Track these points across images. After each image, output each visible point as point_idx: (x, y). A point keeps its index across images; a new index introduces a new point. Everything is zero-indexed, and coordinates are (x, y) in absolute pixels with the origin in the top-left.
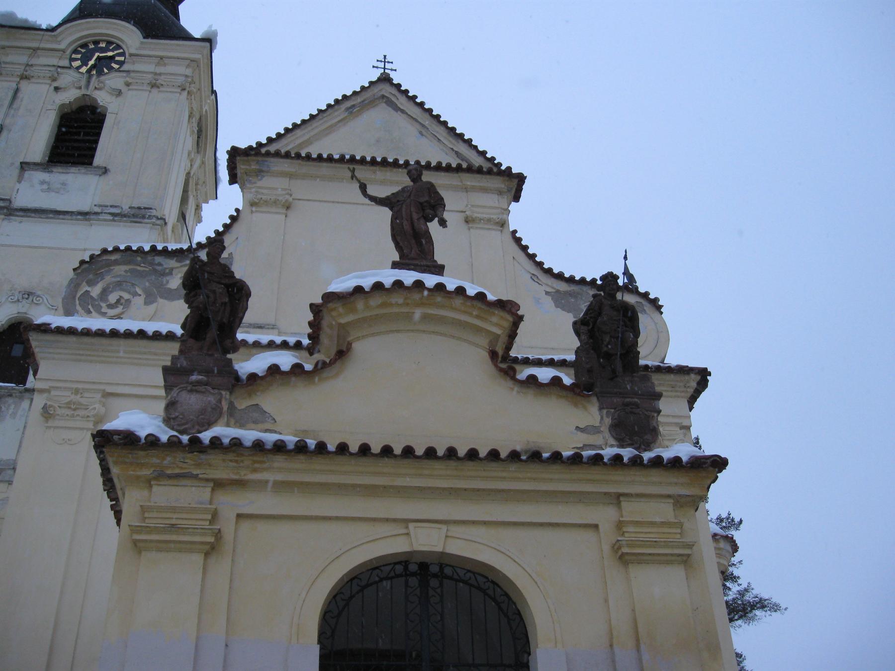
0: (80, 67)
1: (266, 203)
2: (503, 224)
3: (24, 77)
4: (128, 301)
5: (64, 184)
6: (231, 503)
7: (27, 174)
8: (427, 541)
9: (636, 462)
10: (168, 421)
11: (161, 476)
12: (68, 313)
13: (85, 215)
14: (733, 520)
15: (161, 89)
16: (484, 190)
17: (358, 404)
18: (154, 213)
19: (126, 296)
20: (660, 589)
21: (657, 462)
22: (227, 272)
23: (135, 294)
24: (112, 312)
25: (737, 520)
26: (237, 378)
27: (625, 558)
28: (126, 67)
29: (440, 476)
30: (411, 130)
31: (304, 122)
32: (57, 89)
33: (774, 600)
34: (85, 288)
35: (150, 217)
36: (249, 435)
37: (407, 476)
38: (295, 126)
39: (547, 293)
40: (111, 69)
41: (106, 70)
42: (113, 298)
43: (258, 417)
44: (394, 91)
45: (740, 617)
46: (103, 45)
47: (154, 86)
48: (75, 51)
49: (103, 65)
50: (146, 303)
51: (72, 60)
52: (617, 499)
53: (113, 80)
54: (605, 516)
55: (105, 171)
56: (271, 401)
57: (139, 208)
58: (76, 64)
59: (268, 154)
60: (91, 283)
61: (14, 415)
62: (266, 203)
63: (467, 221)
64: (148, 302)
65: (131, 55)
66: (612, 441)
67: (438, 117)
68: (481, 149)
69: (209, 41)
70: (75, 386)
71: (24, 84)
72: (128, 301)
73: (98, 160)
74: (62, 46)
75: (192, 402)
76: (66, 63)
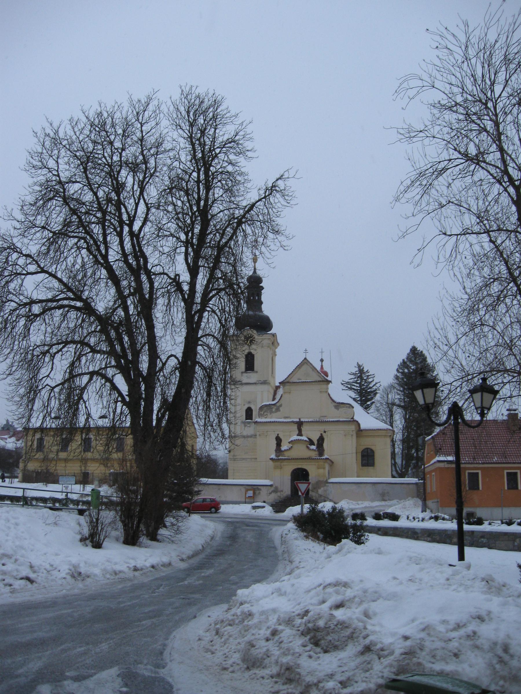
2: (327, 392)
6: (282, 464)
8: (300, 467)
10: (276, 456)
13: (255, 384)
17: (293, 454)
43: (284, 455)
49: (251, 341)
53: (253, 346)
54: (317, 464)
55: (257, 372)
73: (255, 369)
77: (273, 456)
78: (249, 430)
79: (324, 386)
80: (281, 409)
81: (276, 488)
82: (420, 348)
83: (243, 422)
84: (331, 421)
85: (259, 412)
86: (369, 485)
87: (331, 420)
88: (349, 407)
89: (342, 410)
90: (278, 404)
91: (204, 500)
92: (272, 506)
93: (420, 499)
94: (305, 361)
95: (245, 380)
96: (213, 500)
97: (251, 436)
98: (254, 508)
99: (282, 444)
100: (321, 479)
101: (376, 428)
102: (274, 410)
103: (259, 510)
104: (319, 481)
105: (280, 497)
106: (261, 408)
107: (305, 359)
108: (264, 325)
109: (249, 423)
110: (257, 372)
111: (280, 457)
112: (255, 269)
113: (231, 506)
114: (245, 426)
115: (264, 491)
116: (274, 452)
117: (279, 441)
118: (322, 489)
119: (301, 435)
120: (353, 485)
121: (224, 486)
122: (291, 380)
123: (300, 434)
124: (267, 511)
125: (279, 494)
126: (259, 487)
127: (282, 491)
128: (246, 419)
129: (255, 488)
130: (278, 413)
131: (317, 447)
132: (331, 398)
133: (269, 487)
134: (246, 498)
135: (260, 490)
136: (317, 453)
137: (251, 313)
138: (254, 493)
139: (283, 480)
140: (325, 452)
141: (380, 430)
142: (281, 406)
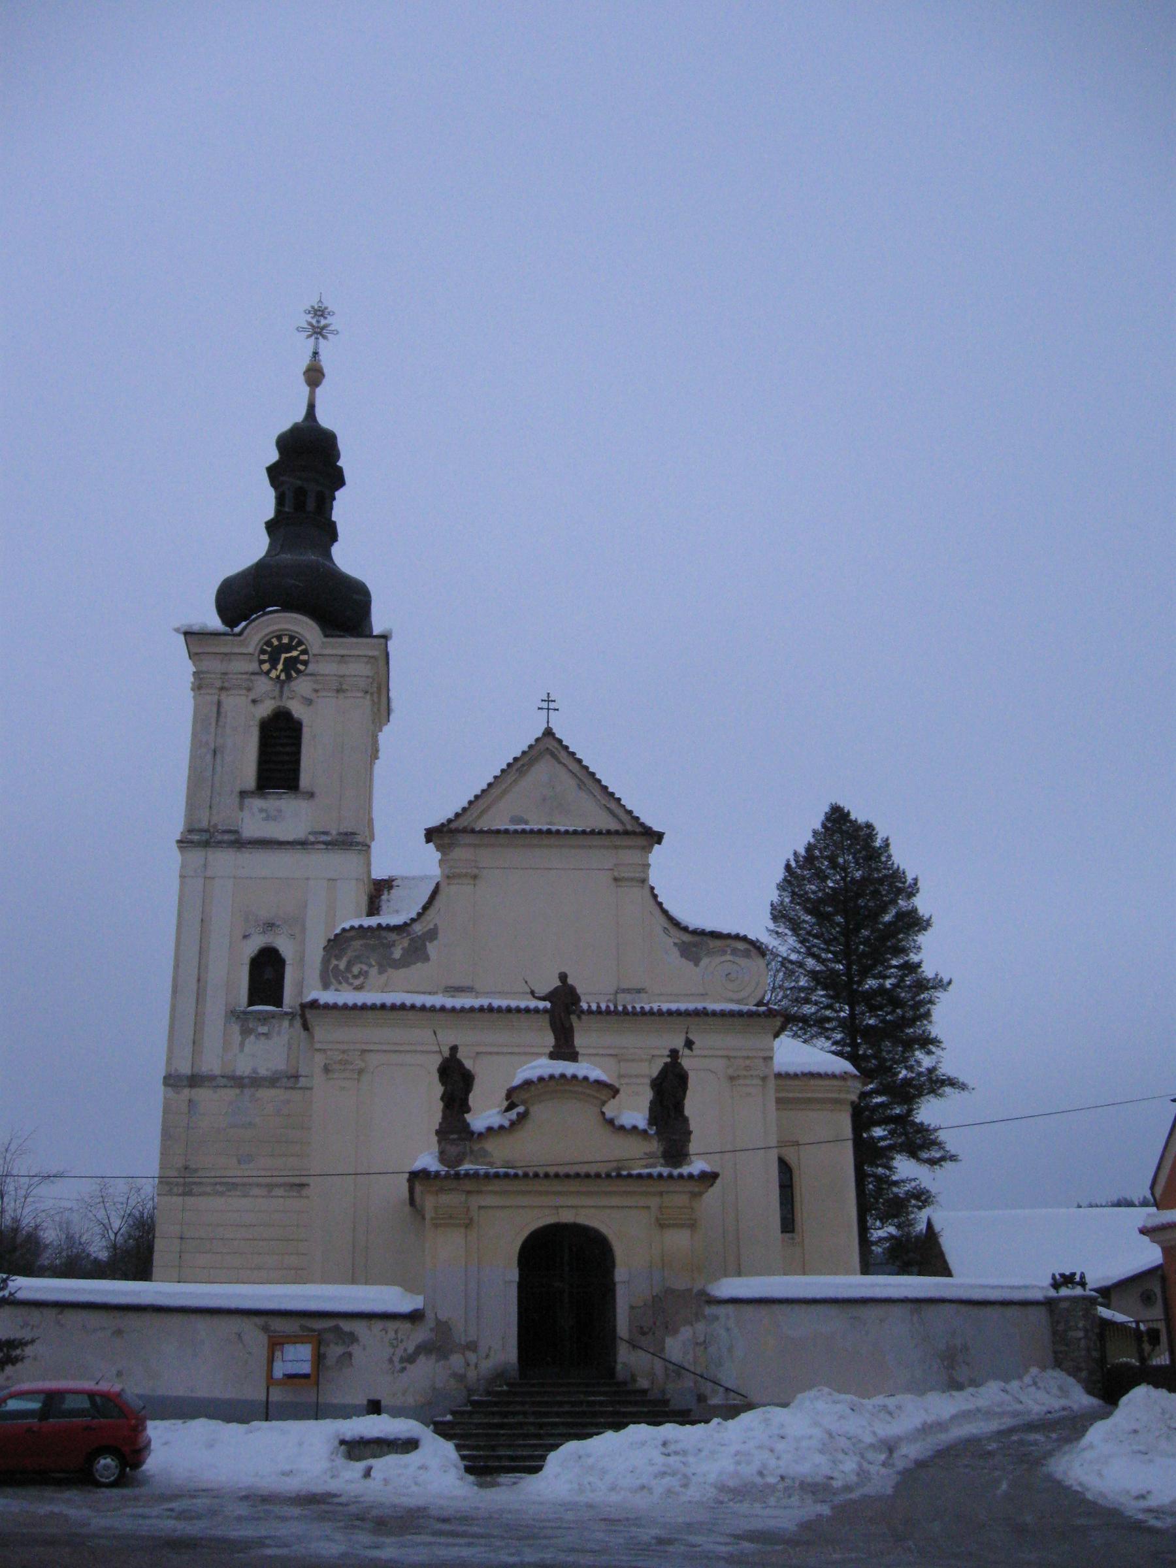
0: (268, 673)
1: (459, 876)
2: (644, 881)
3: (222, 689)
4: (366, 972)
5: (280, 811)
6: (476, 1201)
7: (248, 801)
8: (567, 1217)
9: (670, 1176)
10: (443, 1157)
11: (441, 1190)
12: (326, 986)
13: (302, 844)
14: (941, 981)
15: (349, 694)
16: (629, 847)
18: (359, 839)
19: (365, 968)
20: (678, 1240)
21: (681, 1176)
22: (460, 1064)
23: (371, 966)
24: (357, 982)
25: (946, 980)
26: (472, 1133)
27: (662, 1225)
28: (311, 668)
29: (574, 1186)
30: (572, 783)
31: (483, 791)
32: (254, 701)
33: (961, 1080)
34: (335, 962)
35: (358, 844)
36: (482, 1169)
37: (557, 1186)
38: (477, 797)
39: (675, 944)
40: (299, 672)
41: (294, 675)
42: (356, 970)
44: (556, 745)
45: (929, 1093)
46: (285, 640)
47: (338, 691)
48: (263, 652)
49: (291, 664)
50: (380, 973)
51: (262, 662)
52: (661, 1194)
53: (302, 686)
54: (654, 1202)
55: (311, 795)
56: (490, 1145)
57: (346, 834)
58: (266, 667)
59: (457, 831)
60: (338, 958)
61: (279, 1033)
62: (459, 876)
63: (616, 879)
64: (381, 972)
65: (315, 655)
66: (662, 1161)
67: (593, 774)
68: (629, 808)
69: (385, 637)
70: (342, 1047)
71: (223, 697)
72: (366, 972)
73: (305, 781)
74: (251, 650)
75: (453, 1150)
76: (254, 666)
77: (428, 1160)
78: (267, 1052)
79: (630, 857)
80: (431, 948)
81: (443, 1328)
82: (859, 815)
83: (234, 1014)
84: (670, 1013)
85: (326, 961)
86: (897, 1311)
87: (665, 1007)
88: (746, 954)
89: (714, 965)
90: (418, 928)
91: (52, 1399)
92: (443, 1430)
93: (1074, 1372)
94: (548, 747)
95: (252, 827)
96: (107, 1405)
97: (273, 1081)
98: (356, 1448)
99: (472, 1099)
100: (680, 1283)
101: (798, 1070)
102: (397, 953)
103: (386, 1465)
104: (669, 1291)
105: (461, 1378)
106: (337, 944)
107: (549, 733)
108: (343, 609)
109: (264, 1018)
110: (311, 795)
111: (466, 1167)
112: (311, 407)
113: (201, 1427)
114: (246, 1032)
115: (373, 1346)
116: (434, 1139)
117: (456, 1080)
118: (686, 1332)
119: (573, 1057)
120: (833, 1310)
121: (147, 1317)
122: (484, 824)
123: (564, 1049)
124: (433, 1471)
125: (456, 1360)
126: (347, 1326)
127: (472, 1346)
128: (251, 1003)
129: (325, 1330)
130: (418, 971)
131: (653, 1120)
132: (665, 912)
133: (407, 1325)
134: (270, 1380)
135: (352, 1338)
136: (654, 1146)
137: (287, 557)
138: (319, 1359)
139: (478, 1285)
140: (693, 1147)
141: (819, 1076)
142: (432, 934)
